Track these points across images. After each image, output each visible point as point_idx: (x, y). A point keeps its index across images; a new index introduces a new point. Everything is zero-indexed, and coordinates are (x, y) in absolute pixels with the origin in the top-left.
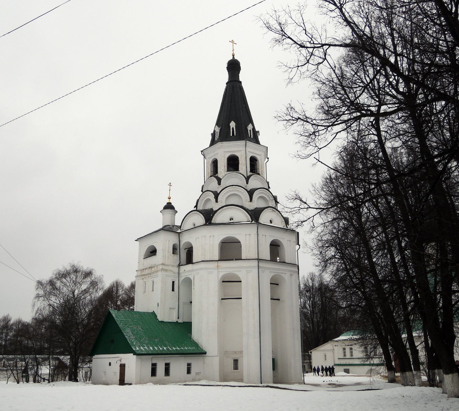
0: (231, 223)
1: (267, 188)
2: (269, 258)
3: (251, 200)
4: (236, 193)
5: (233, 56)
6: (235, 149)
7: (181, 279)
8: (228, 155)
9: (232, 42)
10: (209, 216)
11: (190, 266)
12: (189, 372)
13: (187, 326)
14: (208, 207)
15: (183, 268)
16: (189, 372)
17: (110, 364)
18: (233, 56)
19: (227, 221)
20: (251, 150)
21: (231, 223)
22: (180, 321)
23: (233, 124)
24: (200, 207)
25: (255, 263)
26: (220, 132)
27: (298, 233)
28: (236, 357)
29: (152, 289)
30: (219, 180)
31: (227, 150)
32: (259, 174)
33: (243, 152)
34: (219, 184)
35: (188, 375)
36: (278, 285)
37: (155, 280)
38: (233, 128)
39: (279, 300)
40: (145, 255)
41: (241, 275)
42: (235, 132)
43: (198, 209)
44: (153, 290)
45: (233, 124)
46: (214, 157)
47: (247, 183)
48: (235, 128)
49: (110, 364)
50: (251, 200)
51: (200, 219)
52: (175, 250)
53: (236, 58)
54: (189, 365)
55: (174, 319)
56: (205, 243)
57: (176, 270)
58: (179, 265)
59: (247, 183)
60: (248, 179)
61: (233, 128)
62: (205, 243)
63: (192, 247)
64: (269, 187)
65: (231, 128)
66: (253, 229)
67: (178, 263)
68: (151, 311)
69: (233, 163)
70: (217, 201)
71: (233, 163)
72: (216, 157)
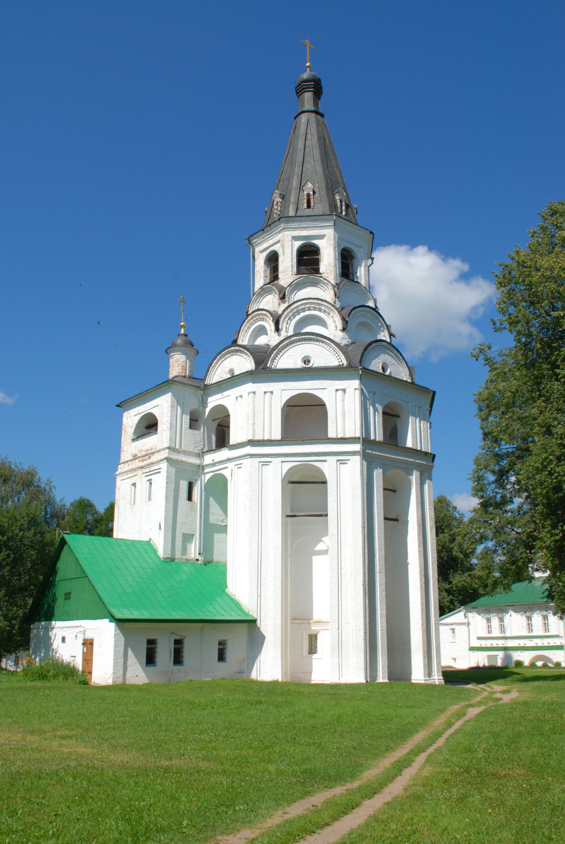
0: (308, 372)
1: (374, 307)
2: (379, 437)
8: (298, 244)
11: (224, 454)
12: (221, 657)
14: (261, 341)
16: (221, 657)
19: (300, 365)
27: (434, 393)
34: (283, 298)
35: (221, 664)
36: (394, 491)
39: (396, 520)
40: (134, 433)
41: (328, 468)
43: (240, 342)
44: (150, 499)
46: (271, 249)
48: (311, 193)
52: (194, 422)
63: (229, 415)
64: (376, 307)
68: (146, 539)
70: (277, 329)
71: (308, 258)
72: (276, 248)
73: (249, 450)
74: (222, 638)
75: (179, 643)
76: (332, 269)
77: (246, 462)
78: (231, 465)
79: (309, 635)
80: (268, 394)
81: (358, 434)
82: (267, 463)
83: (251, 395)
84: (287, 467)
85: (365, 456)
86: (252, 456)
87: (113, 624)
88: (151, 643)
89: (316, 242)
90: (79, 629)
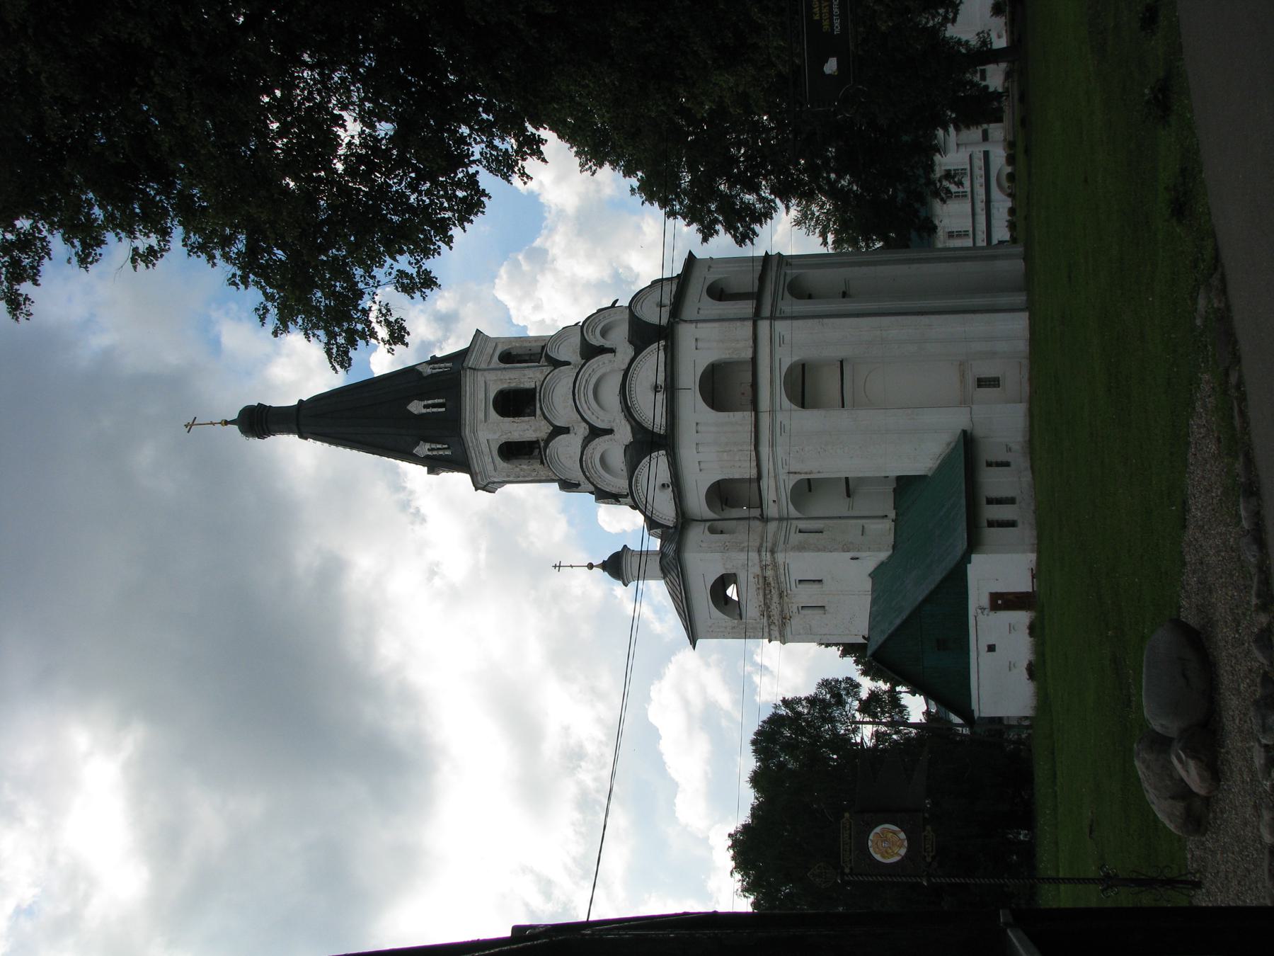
0: (670, 388)
3: (612, 351)
4: (593, 381)
5: (226, 423)
6: (481, 395)
7: (793, 512)
8: (493, 414)
9: (189, 426)
10: (647, 442)
13: (904, 486)
15: (772, 511)
17: (991, 648)
18: (226, 423)
20: (485, 358)
21: (670, 388)
22: (892, 514)
23: (416, 407)
24: (621, 484)
25: (764, 326)
26: (432, 442)
28: (971, 382)
29: (816, 586)
30: (558, 431)
31: (481, 415)
32: (543, 347)
33: (491, 376)
34: (566, 430)
37: (796, 575)
38: (425, 407)
41: (787, 359)
42: (436, 401)
44: (820, 581)
45: (416, 407)
46: (495, 453)
47: (568, 363)
49: (991, 648)
50: (612, 351)
51: (657, 467)
53: (235, 416)
54: (989, 464)
55: (888, 525)
56: (711, 446)
57: (772, 526)
58: (764, 519)
59: (568, 363)
60: (556, 364)
61: (425, 407)
62: (711, 446)
65: (424, 411)
66: (686, 333)
67: (757, 524)
69: (514, 403)
71: (514, 403)
73: (765, 450)
74: (984, 501)
75: (990, 501)
76: (529, 373)
77: (780, 451)
78: (782, 476)
79: (979, 386)
80: (700, 428)
81: (749, 324)
82: (782, 428)
83: (701, 449)
84: (786, 403)
85: (772, 318)
86: (773, 445)
87: (974, 556)
88: (991, 524)
89: (492, 395)
90: (980, 617)
